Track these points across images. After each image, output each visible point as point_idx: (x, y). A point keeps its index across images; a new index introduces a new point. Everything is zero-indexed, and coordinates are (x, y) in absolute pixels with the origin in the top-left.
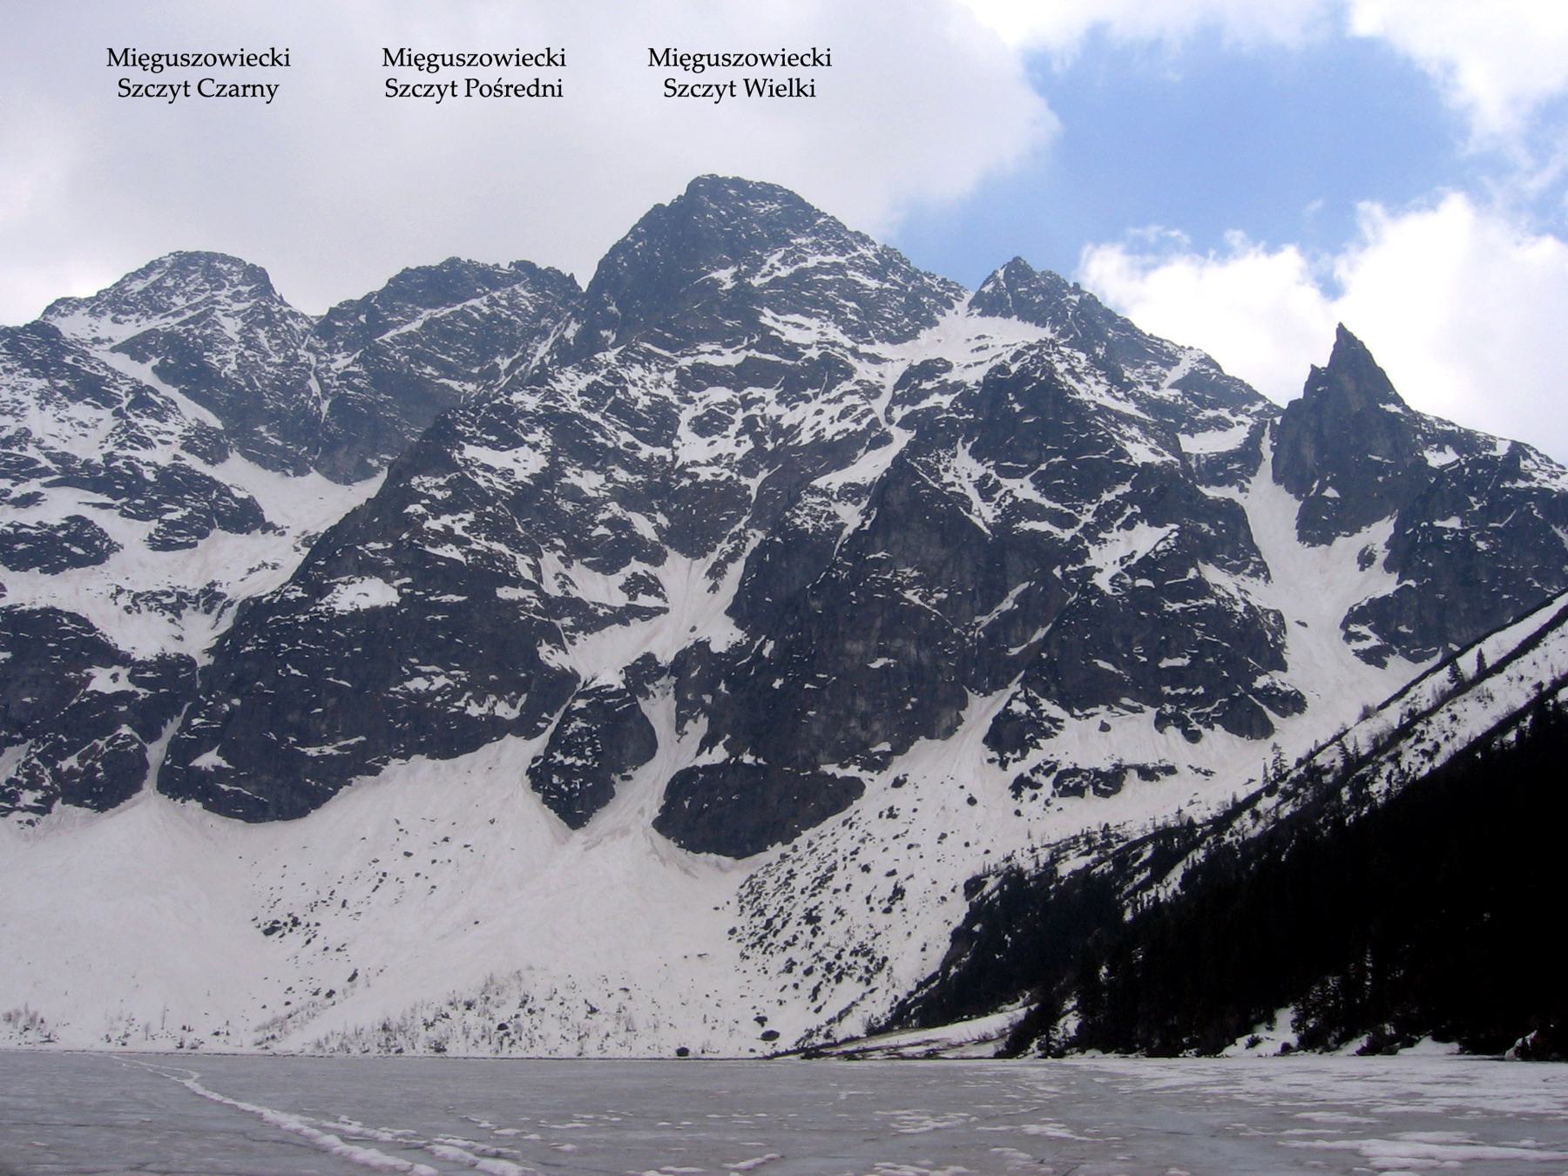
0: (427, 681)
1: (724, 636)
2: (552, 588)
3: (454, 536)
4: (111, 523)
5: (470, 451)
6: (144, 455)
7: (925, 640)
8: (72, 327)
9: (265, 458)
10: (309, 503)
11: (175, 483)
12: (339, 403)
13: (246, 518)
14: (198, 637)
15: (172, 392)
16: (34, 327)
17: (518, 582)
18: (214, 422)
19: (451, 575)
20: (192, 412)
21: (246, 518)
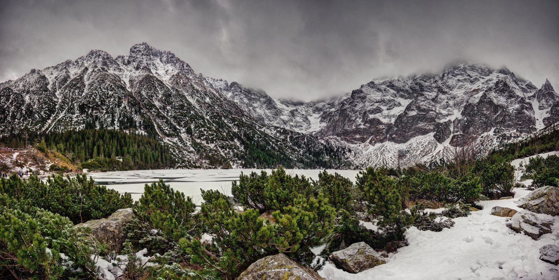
0: (421, 125)
1: (460, 117)
2: (437, 111)
3: (424, 104)
4: (382, 107)
5: (426, 93)
6: (385, 98)
7: (486, 118)
8: (376, 82)
9: (402, 96)
10: (405, 103)
11: (390, 101)
12: (411, 88)
13: (400, 105)
14: (393, 121)
15: (388, 88)
16: (371, 82)
17: (432, 111)
18: (395, 92)
19: (424, 110)
20: (392, 91)
21: (400, 105)
